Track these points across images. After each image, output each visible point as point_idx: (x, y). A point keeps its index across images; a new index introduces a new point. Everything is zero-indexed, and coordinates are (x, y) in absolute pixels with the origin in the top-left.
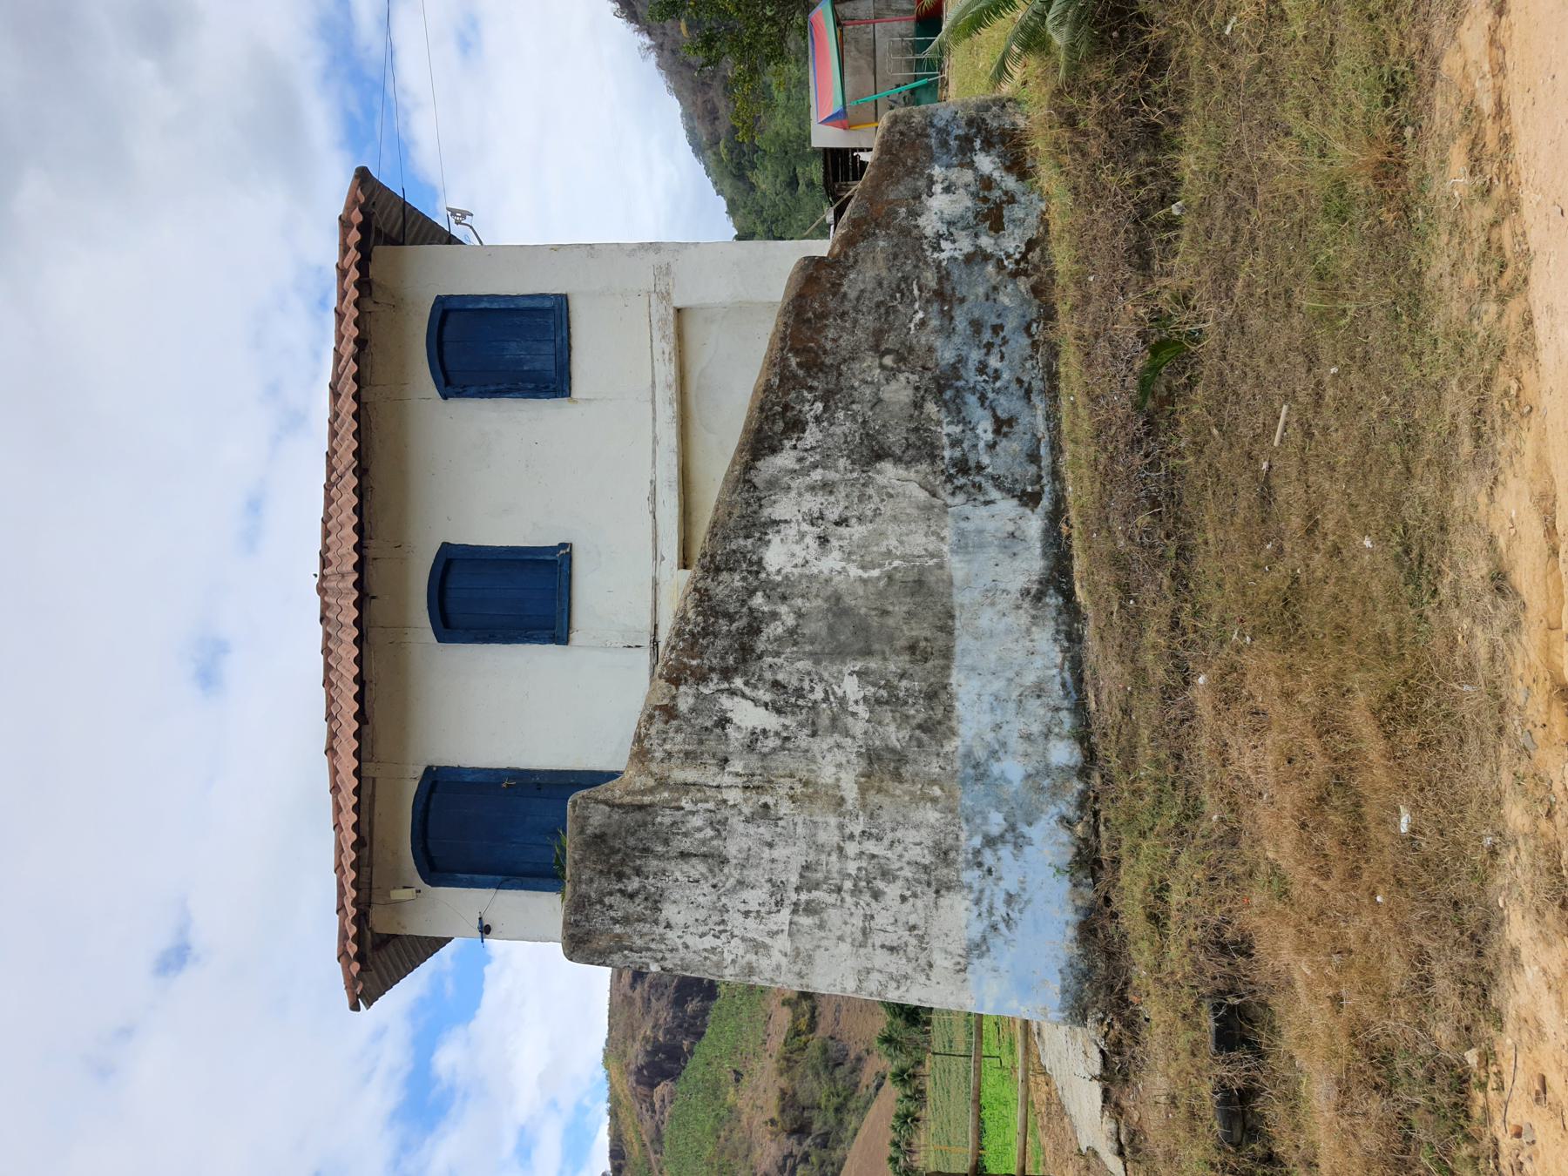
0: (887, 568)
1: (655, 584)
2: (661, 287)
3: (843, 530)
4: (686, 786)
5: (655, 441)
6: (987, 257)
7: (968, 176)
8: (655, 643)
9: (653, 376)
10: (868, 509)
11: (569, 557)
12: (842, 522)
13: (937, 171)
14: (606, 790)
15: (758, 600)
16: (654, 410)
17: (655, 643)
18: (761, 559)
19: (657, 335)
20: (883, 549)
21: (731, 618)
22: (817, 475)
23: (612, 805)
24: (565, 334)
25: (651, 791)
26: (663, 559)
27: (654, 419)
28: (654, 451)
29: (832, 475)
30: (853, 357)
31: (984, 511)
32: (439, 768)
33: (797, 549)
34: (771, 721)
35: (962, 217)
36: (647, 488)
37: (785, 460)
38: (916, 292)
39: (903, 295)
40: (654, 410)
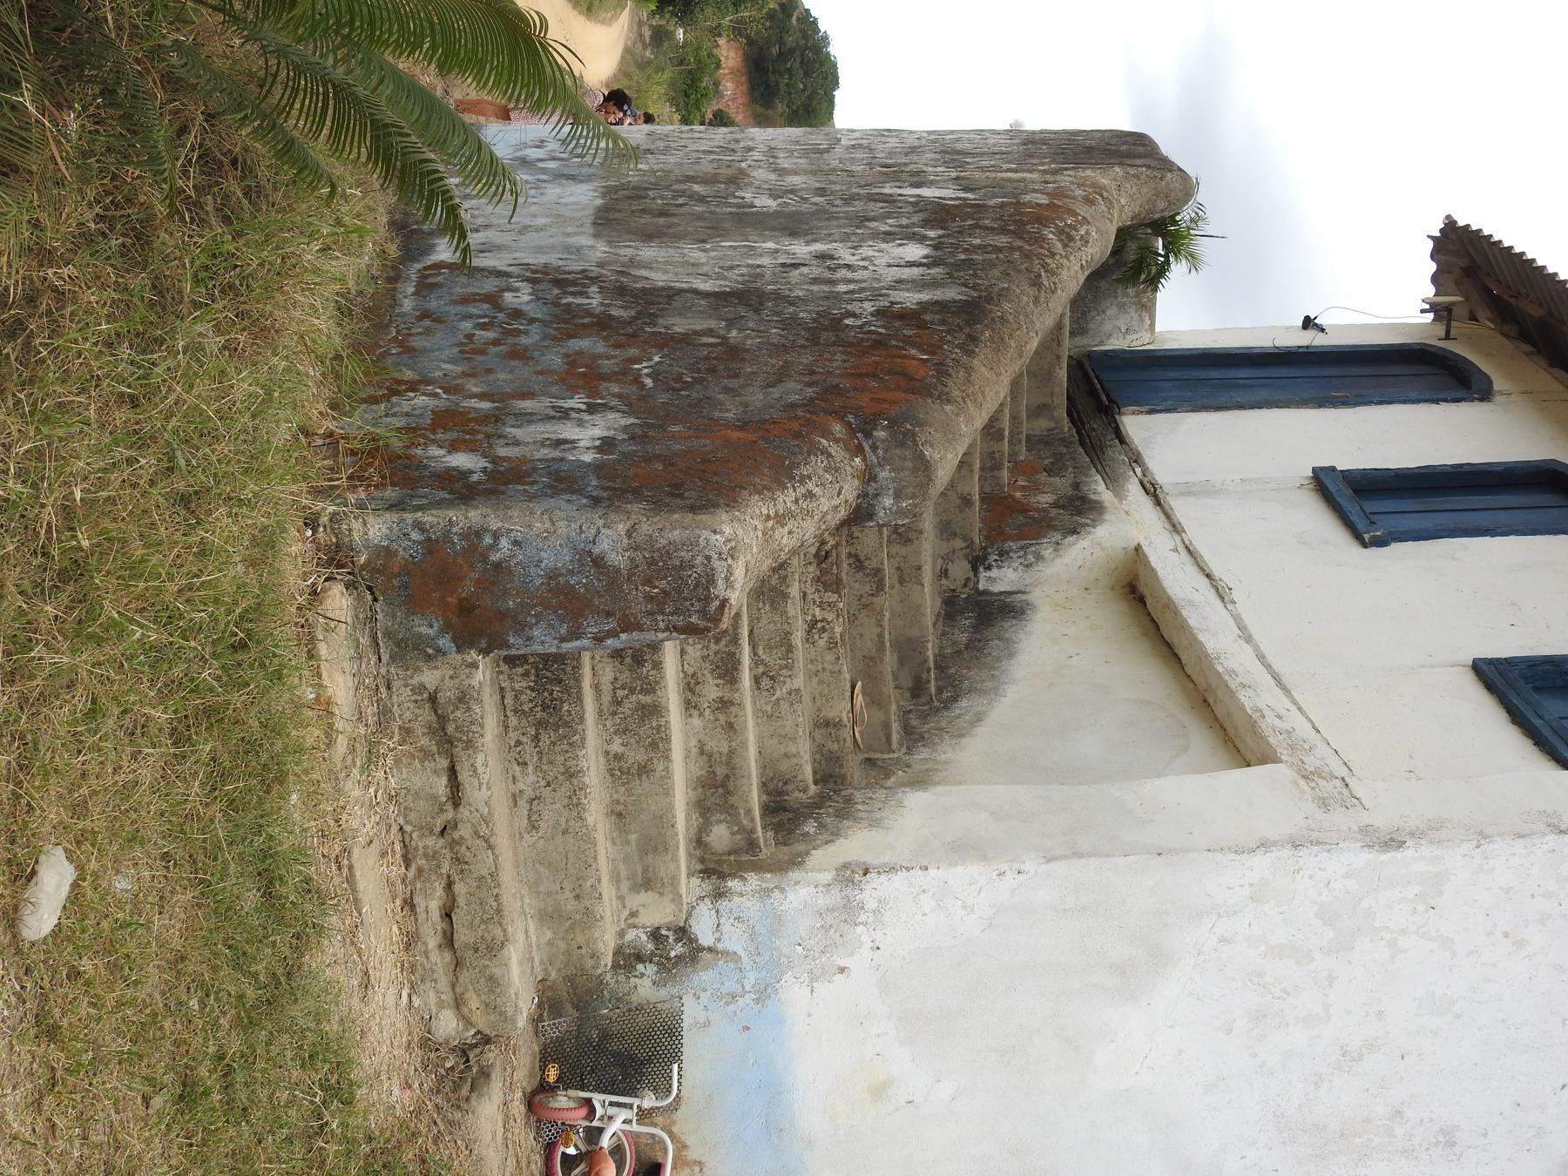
0: (708, 246)
1: (1176, 528)
2: (1330, 788)
3: (789, 261)
4: (1009, 170)
5: (1249, 639)
6: (482, 396)
7: (503, 452)
8: (1152, 491)
9: (1294, 702)
10: (744, 270)
11: (1358, 536)
12: (795, 266)
13: (588, 458)
14: (1136, 176)
15: (932, 234)
16: (1268, 667)
17: (1152, 491)
18: (936, 247)
19: (1303, 729)
20: (712, 254)
21: (977, 226)
22: (842, 288)
23: (1120, 164)
24: (1538, 722)
25: (1066, 169)
26: (1176, 550)
27: (1261, 658)
28: (1242, 628)
29: (815, 288)
30: (782, 349)
31: (530, 261)
32: (1472, 401)
33: (870, 253)
34: (887, 191)
35: (530, 422)
36: (1235, 595)
37: (910, 298)
38: (649, 382)
39: (679, 378)
40: (1268, 667)
